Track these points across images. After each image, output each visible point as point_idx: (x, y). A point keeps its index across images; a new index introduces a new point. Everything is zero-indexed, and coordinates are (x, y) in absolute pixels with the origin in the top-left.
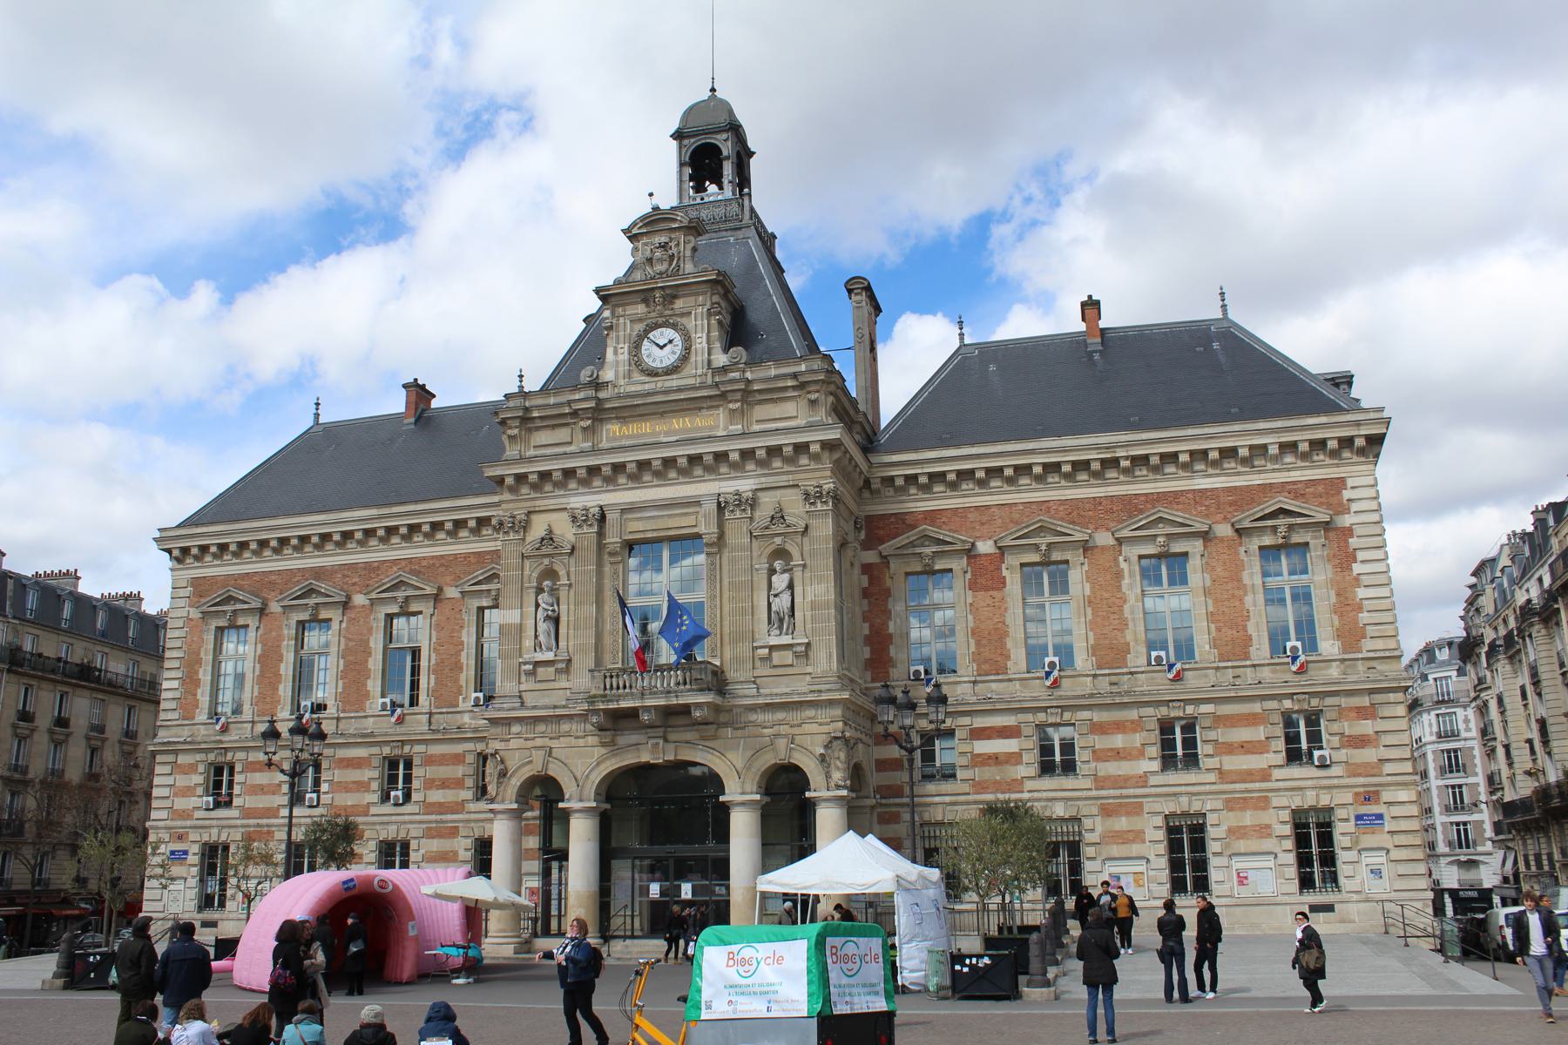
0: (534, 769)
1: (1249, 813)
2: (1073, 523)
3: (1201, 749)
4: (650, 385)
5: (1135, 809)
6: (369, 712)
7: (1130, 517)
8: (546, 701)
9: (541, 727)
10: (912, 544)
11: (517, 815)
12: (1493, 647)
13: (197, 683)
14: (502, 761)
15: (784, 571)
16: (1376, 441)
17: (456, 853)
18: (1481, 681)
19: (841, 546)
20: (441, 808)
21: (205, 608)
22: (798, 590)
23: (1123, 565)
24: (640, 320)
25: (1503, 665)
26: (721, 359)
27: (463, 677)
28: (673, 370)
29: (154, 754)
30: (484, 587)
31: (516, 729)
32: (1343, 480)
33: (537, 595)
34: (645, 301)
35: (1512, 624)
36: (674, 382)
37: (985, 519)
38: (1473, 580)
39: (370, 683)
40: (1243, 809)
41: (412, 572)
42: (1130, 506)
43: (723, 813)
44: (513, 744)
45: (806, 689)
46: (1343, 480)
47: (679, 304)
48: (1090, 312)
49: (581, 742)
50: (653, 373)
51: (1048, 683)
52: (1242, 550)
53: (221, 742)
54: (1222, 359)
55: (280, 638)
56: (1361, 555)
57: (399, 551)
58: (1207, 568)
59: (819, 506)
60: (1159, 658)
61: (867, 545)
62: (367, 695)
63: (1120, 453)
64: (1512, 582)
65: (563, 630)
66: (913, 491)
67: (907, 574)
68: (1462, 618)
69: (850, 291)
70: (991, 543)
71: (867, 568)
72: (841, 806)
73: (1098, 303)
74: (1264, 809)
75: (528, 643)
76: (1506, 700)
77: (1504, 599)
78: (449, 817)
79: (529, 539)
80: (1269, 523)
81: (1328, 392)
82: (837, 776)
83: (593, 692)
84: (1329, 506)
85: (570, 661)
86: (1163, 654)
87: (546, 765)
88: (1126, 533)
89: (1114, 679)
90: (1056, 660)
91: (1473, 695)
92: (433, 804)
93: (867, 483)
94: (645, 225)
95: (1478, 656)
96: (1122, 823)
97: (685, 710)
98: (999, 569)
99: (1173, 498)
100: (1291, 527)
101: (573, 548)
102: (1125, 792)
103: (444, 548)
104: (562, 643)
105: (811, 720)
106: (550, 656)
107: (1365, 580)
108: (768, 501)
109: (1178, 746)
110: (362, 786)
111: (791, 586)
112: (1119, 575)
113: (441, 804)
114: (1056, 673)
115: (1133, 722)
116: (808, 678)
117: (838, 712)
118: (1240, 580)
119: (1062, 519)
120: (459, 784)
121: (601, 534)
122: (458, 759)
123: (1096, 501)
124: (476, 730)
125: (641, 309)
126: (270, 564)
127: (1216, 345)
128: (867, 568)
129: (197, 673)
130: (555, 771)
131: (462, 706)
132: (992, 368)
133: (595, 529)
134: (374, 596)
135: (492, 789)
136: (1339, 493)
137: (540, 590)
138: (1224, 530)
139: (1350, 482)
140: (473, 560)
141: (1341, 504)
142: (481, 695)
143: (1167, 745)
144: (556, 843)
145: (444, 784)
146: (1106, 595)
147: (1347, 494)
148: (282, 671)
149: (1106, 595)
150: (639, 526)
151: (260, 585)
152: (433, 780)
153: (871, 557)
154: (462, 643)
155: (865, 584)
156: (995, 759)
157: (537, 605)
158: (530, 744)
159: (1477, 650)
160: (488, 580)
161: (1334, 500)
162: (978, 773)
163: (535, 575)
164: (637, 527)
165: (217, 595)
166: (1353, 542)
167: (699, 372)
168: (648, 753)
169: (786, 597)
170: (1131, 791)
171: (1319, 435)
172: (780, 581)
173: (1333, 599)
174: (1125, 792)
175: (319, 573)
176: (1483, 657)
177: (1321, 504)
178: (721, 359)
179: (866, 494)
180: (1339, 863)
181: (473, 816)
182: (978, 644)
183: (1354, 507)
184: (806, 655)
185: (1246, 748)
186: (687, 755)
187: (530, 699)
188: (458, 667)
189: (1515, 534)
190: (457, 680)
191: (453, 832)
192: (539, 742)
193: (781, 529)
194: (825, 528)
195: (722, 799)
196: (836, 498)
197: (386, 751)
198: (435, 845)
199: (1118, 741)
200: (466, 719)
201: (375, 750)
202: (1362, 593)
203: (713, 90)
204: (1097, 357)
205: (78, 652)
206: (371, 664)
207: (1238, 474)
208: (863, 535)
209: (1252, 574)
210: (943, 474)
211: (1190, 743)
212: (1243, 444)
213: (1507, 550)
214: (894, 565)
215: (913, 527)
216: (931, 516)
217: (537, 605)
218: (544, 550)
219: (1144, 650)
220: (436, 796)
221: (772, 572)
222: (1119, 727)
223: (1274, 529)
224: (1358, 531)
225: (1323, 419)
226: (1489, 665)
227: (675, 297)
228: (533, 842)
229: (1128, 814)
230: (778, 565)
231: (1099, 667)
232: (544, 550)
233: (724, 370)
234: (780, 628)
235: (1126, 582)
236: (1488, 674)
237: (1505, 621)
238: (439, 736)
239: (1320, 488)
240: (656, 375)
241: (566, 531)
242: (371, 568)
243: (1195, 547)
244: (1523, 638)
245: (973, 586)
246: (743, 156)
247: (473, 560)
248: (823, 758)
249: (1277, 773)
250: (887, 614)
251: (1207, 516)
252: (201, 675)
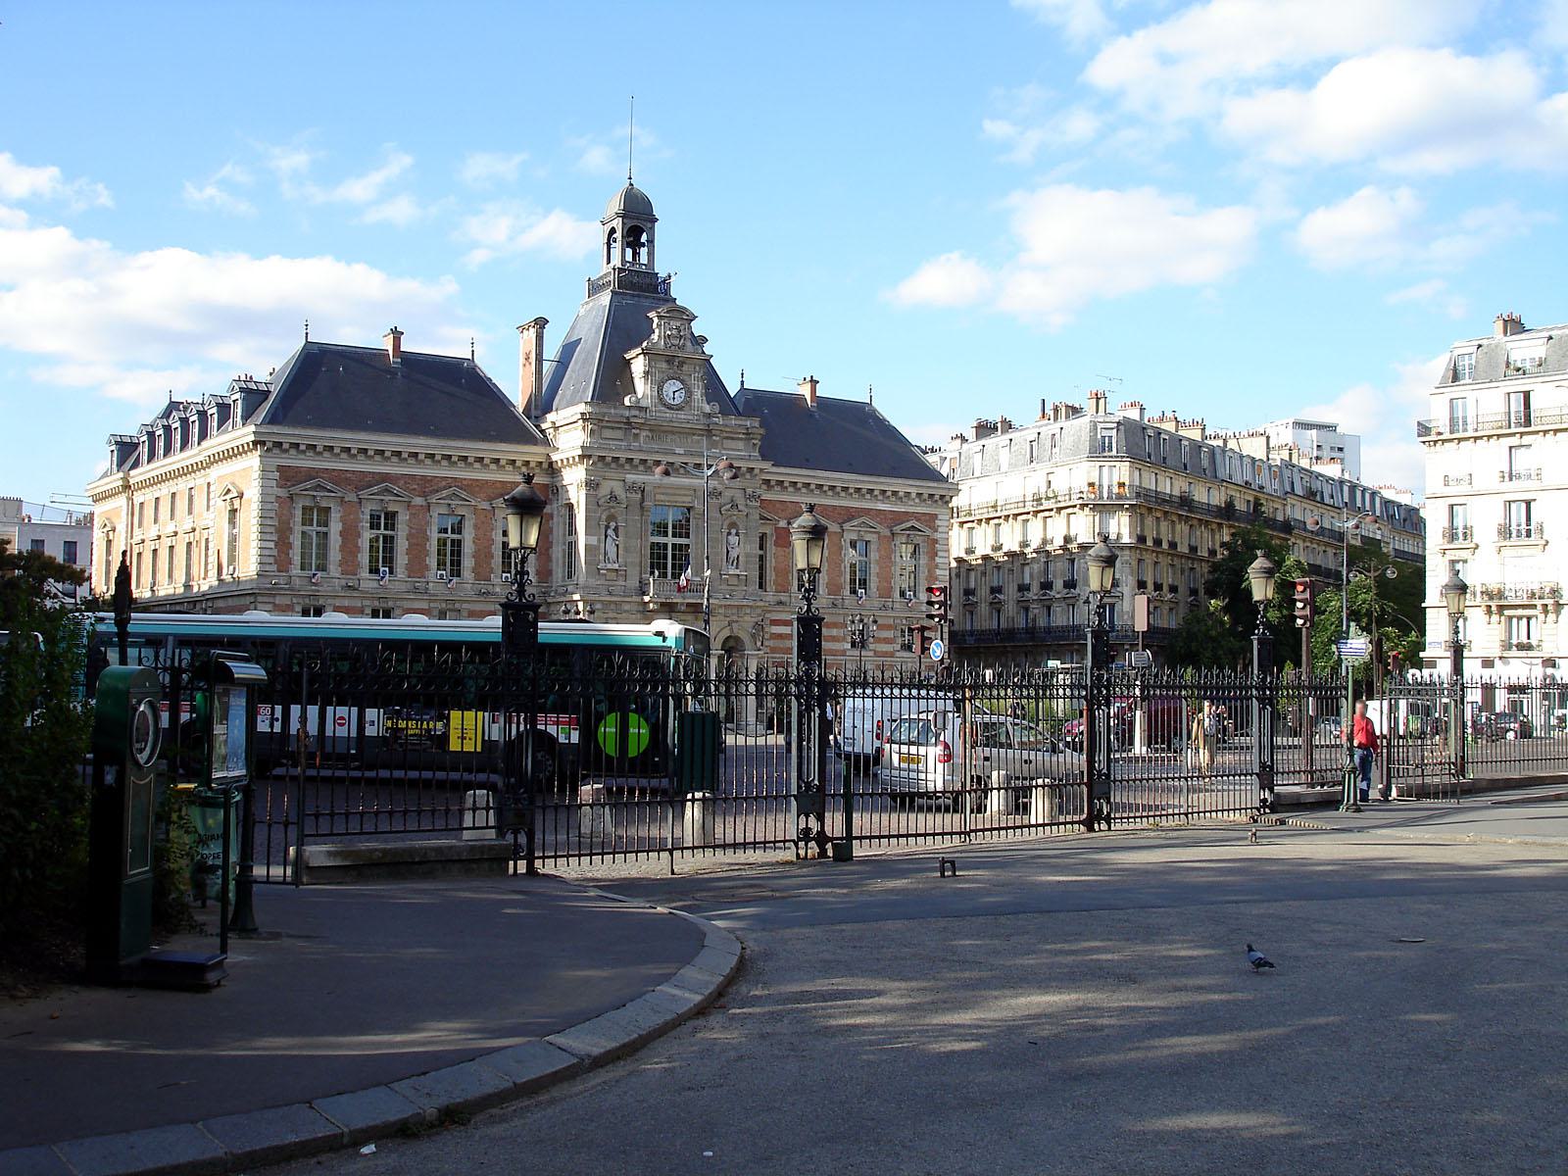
4: (669, 414)
13: (290, 546)
24: (663, 372)
26: (707, 409)
28: (679, 408)
34: (668, 361)
36: (682, 415)
37: (782, 508)
47: (685, 368)
50: (670, 407)
53: (318, 591)
58: (879, 550)
62: (427, 568)
75: (601, 557)
94: (668, 312)
106: (616, 566)
108: (728, 494)
125: (664, 365)
137: (607, 527)
139: (940, 517)
147: (938, 523)
156: (780, 636)
158: (606, 616)
162: (771, 643)
167: (696, 413)
173: (926, 573)
178: (707, 409)
182: (776, 575)
185: (887, 641)
202: (938, 572)
203: (630, 178)
212: (902, 491)
218: (611, 504)
221: (729, 534)
225: (935, 485)
227: (684, 363)
230: (734, 531)
231: (829, 594)
232: (611, 504)
233: (709, 416)
239: (927, 518)
240: (673, 409)
241: (620, 492)
247: (498, 485)
248: (753, 636)
249: (898, 654)
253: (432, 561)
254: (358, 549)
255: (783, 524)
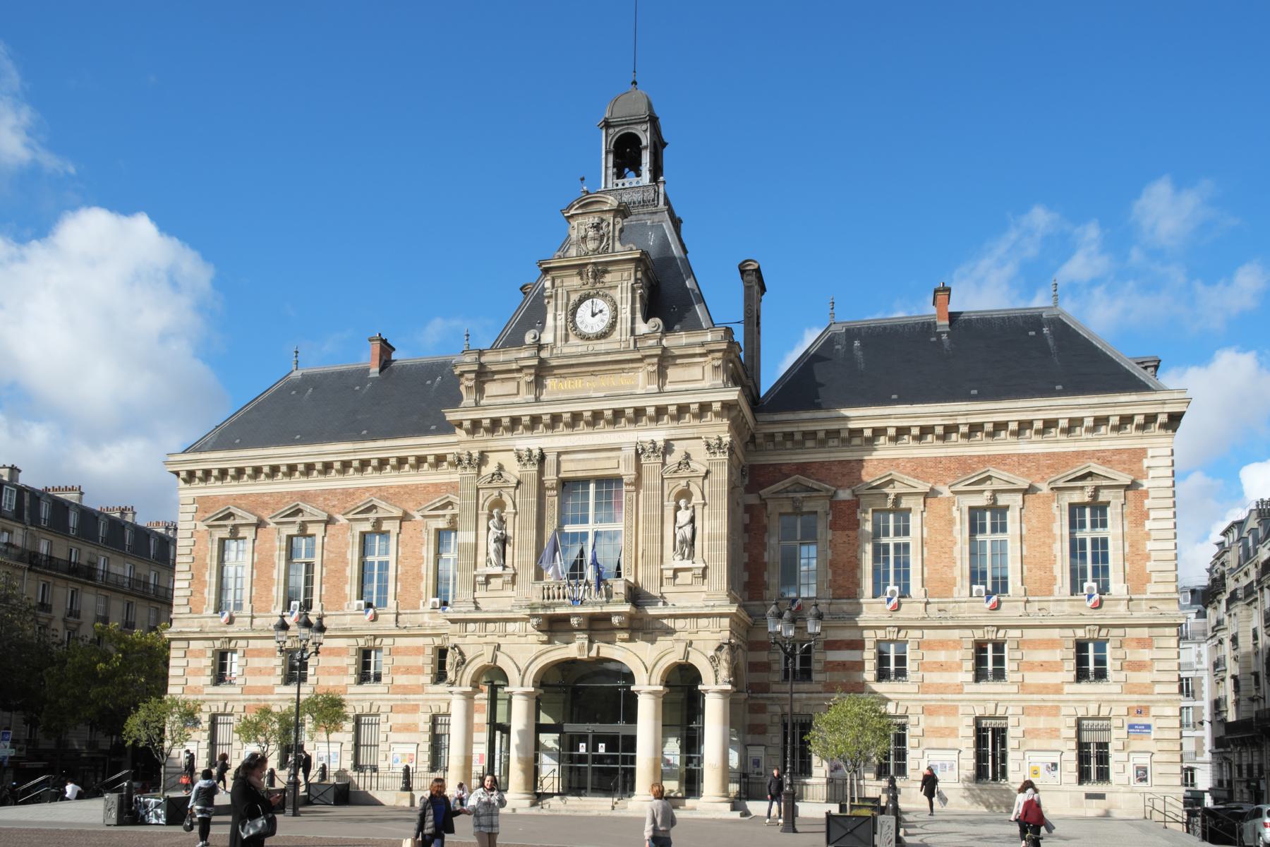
0: (486, 660)
1: (1042, 718)
2: (917, 477)
3: (1008, 666)
5: (952, 711)
6: (348, 611)
7: (964, 474)
8: (495, 607)
9: (491, 626)
10: (786, 490)
11: (469, 697)
12: (1233, 594)
14: (461, 653)
15: (687, 508)
16: (1174, 420)
17: (416, 725)
18: (1219, 622)
19: (732, 489)
20: (405, 690)
21: (209, 522)
22: (698, 523)
23: (956, 514)
25: (1239, 608)
27: (423, 585)
29: (171, 640)
30: (440, 512)
31: (471, 626)
32: (1144, 450)
33: (489, 520)
35: (1253, 576)
38: (1222, 538)
39: (347, 588)
40: (1038, 715)
41: (381, 498)
42: (964, 464)
43: (632, 699)
44: (468, 640)
45: (701, 604)
46: (1144, 450)
48: (942, 297)
49: (523, 640)
51: (889, 607)
52: (1055, 505)
54: (1051, 342)
55: (272, 549)
56: (1152, 514)
57: (371, 479)
59: (718, 456)
60: (979, 591)
61: (749, 490)
62: (345, 597)
63: (961, 420)
64: (1257, 541)
65: (509, 549)
66: (789, 444)
67: (781, 514)
68: (1210, 571)
69: (743, 272)
70: (849, 491)
71: (748, 509)
72: (724, 699)
73: (949, 290)
74: (1056, 715)
76: (1240, 640)
77: (1247, 556)
78: (412, 697)
79: (483, 473)
80: (1079, 484)
81: (1138, 372)
82: (724, 673)
83: (534, 600)
84: (1131, 471)
85: (515, 575)
86: (983, 587)
87: (495, 658)
88: (960, 488)
89: (942, 606)
90: (896, 588)
91: (1210, 634)
92: (399, 686)
93: (753, 437)
95: (1219, 602)
96: (941, 721)
97: (607, 617)
98: (855, 513)
99: (1000, 460)
100: (1097, 489)
101: (519, 483)
102: (944, 696)
103: (408, 478)
104: (508, 561)
105: (706, 629)
106: (499, 570)
107: (1154, 535)
109: (987, 661)
110: (342, 671)
111: (692, 520)
112: (951, 522)
113: (405, 687)
114: (895, 600)
115: (954, 641)
116: (704, 595)
117: (726, 622)
118: (1050, 530)
119: (908, 474)
120: (420, 670)
121: (541, 472)
122: (419, 651)
123: (937, 460)
124: (433, 628)
126: (263, 487)
127: (1045, 330)
128: (748, 509)
129: (203, 575)
130: (503, 662)
131: (422, 609)
132: (857, 343)
133: (536, 468)
134: (350, 516)
135: (451, 675)
136: (1140, 461)
137: (491, 517)
138: (1045, 488)
139: (1150, 453)
140: (431, 489)
141: (1141, 470)
142: (437, 600)
143: (980, 660)
144: (501, 719)
145: (408, 671)
146: (940, 538)
147: (1146, 463)
148: (275, 576)
149: (940, 538)
150: (571, 466)
151: (255, 502)
152: (399, 667)
153: (752, 499)
154: (422, 558)
155: (747, 521)
157: (489, 529)
159: (1219, 597)
160: (444, 507)
161: (1135, 467)
163: (487, 504)
164: (572, 468)
165: (219, 510)
166: (1148, 503)
168: (575, 649)
169: (688, 530)
170: (950, 697)
171: (1128, 411)
172: (684, 516)
174: (944, 696)
175: (304, 496)
176: (1224, 603)
177: (1123, 470)
179: (751, 447)
180: (1111, 761)
181: (431, 697)
183: (1151, 473)
184: (704, 576)
186: (607, 651)
187: (482, 603)
188: (418, 577)
189: (1262, 501)
190: (418, 588)
191: (415, 709)
192: (489, 639)
193: (685, 473)
194: (721, 475)
195: (633, 688)
196: (731, 450)
197: (361, 642)
198: (397, 719)
199: (941, 656)
200: (426, 618)
201: (353, 642)
204: (944, 337)
205: (83, 554)
206: (348, 572)
207: (1057, 441)
208: (747, 481)
209: (1061, 527)
210: (815, 433)
211: (999, 661)
213: (1254, 514)
214: (771, 505)
215: (788, 476)
216: (803, 468)
217: (489, 529)
219: (968, 584)
220: (401, 680)
221: (678, 508)
222: (943, 645)
223: (1082, 488)
224: (1152, 494)
226: (1228, 609)
228: (481, 718)
229: (946, 714)
230: (682, 503)
232: (494, 484)
234: (683, 555)
235: (957, 527)
236: (1226, 618)
237: (1246, 574)
238: (405, 632)
239: (1125, 457)
241: (514, 470)
242: (348, 493)
243: (1014, 501)
244: (1262, 590)
245: (833, 526)
246: (658, 146)
247: (431, 489)
248: (713, 659)
250: (764, 546)
251: (1028, 476)
252: (207, 577)
253: (351, 589)
254: (271, 578)
255: (845, 495)
